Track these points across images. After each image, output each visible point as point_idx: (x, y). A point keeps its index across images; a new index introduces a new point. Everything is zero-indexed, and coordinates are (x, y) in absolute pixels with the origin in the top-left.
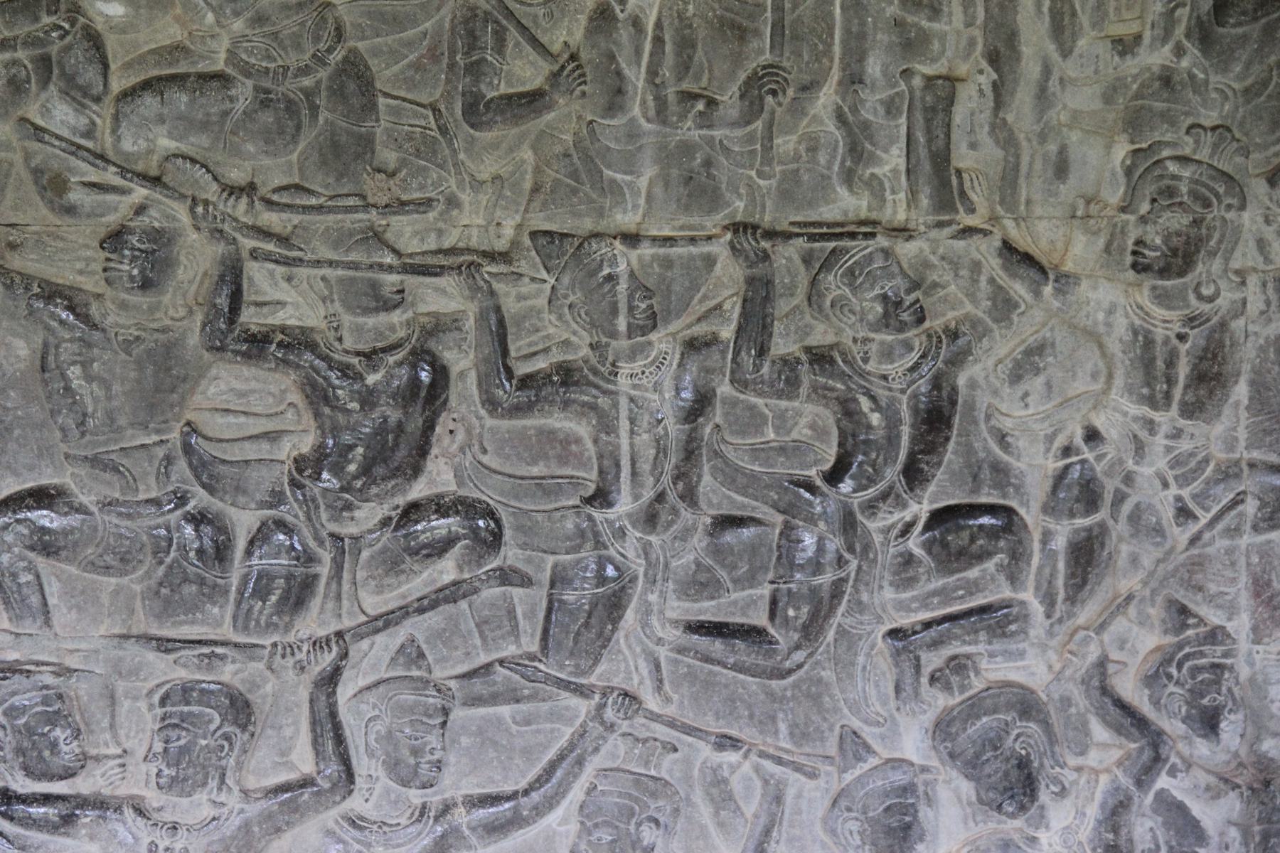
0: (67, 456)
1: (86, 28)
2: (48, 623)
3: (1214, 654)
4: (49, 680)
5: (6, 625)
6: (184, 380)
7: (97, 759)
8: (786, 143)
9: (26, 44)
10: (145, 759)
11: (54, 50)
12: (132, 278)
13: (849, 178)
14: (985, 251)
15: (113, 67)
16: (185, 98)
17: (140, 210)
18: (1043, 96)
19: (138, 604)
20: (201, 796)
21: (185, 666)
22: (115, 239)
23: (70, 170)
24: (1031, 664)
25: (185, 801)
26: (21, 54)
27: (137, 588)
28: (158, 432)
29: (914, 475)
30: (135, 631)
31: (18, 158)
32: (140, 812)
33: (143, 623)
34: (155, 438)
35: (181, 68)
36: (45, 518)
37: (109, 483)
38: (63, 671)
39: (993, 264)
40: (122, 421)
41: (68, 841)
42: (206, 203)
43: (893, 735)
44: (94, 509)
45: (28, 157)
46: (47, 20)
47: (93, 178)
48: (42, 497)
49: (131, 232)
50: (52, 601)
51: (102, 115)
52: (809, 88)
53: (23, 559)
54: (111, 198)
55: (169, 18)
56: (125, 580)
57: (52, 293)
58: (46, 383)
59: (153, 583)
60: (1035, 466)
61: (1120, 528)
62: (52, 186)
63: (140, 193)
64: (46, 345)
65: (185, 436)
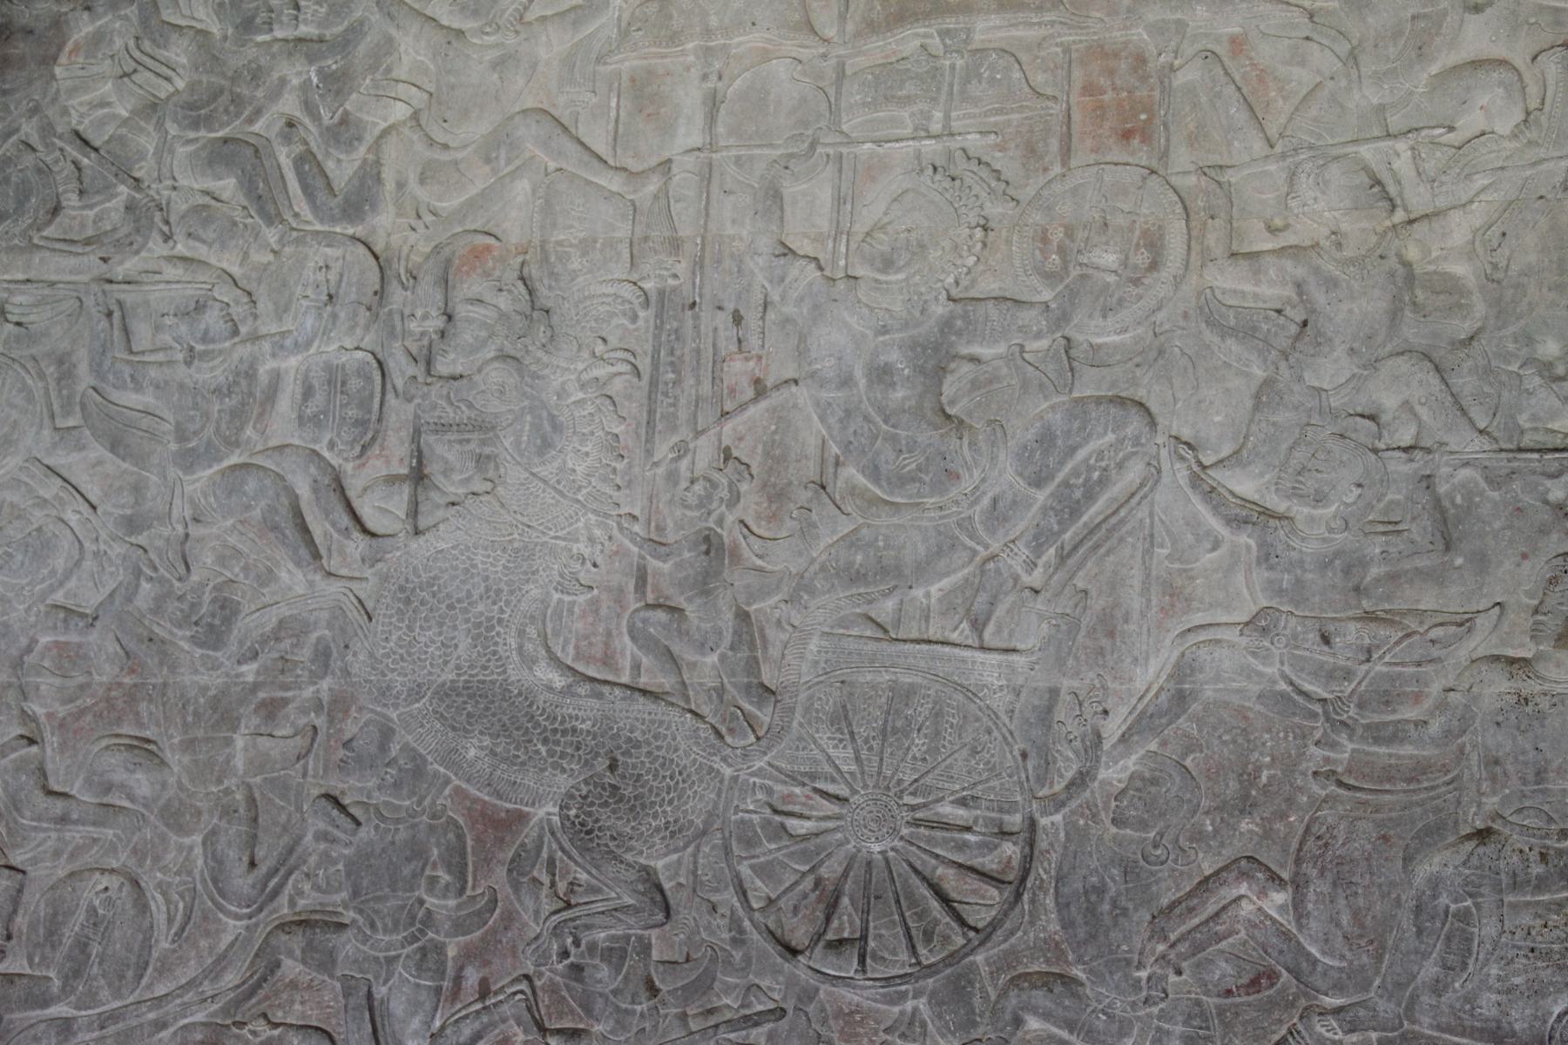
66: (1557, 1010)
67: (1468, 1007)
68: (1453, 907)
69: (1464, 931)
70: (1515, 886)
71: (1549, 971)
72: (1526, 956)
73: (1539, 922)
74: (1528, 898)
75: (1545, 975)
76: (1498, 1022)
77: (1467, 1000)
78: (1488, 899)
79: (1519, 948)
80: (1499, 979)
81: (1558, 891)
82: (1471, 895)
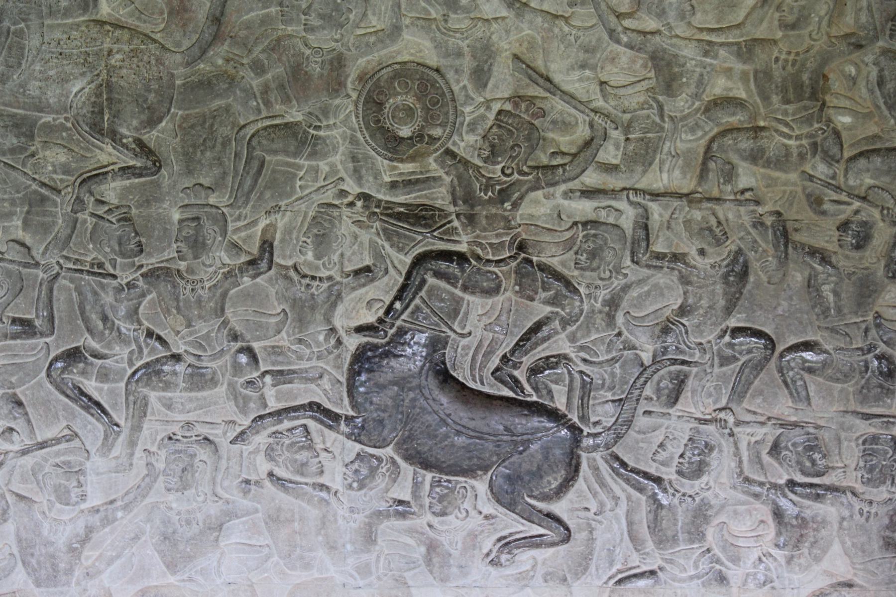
0: (819, 327)
1: (834, 129)
2: (809, 404)
4: (812, 430)
5: (791, 404)
6: (876, 291)
7: (833, 468)
9: (806, 137)
10: (855, 469)
11: (819, 140)
12: (852, 244)
15: (845, 146)
16: (879, 160)
17: (857, 212)
19: (851, 397)
20: (883, 488)
21: (875, 426)
22: (844, 226)
23: (825, 195)
25: (875, 490)
26: (804, 142)
27: (851, 389)
28: (862, 316)
30: (850, 409)
31: (799, 189)
32: (854, 494)
33: (853, 406)
34: (861, 319)
35: (878, 146)
36: (808, 355)
37: (838, 340)
38: (818, 427)
40: (846, 311)
41: (821, 506)
42: (888, 209)
44: (832, 352)
45: (804, 189)
46: (816, 126)
47: (835, 198)
48: (807, 346)
49: (852, 222)
50: (811, 394)
51: (840, 169)
53: (798, 374)
54: (842, 207)
55: (872, 123)
56: (845, 385)
57: (813, 252)
58: (809, 293)
59: (859, 387)
62: (815, 202)
63: (857, 204)
64: (810, 275)
65: (876, 318)
66: (75, 90)
67: (21, 90)
68: (13, 28)
69: (19, 43)
70: (51, 14)
71: (70, 66)
72: (57, 58)
73: (65, 36)
74: (59, 21)
75: (68, 69)
76: (40, 98)
77: (21, 86)
78: (34, 23)
79: (53, 53)
80: (41, 72)
81: (77, 17)
82: (24, 20)
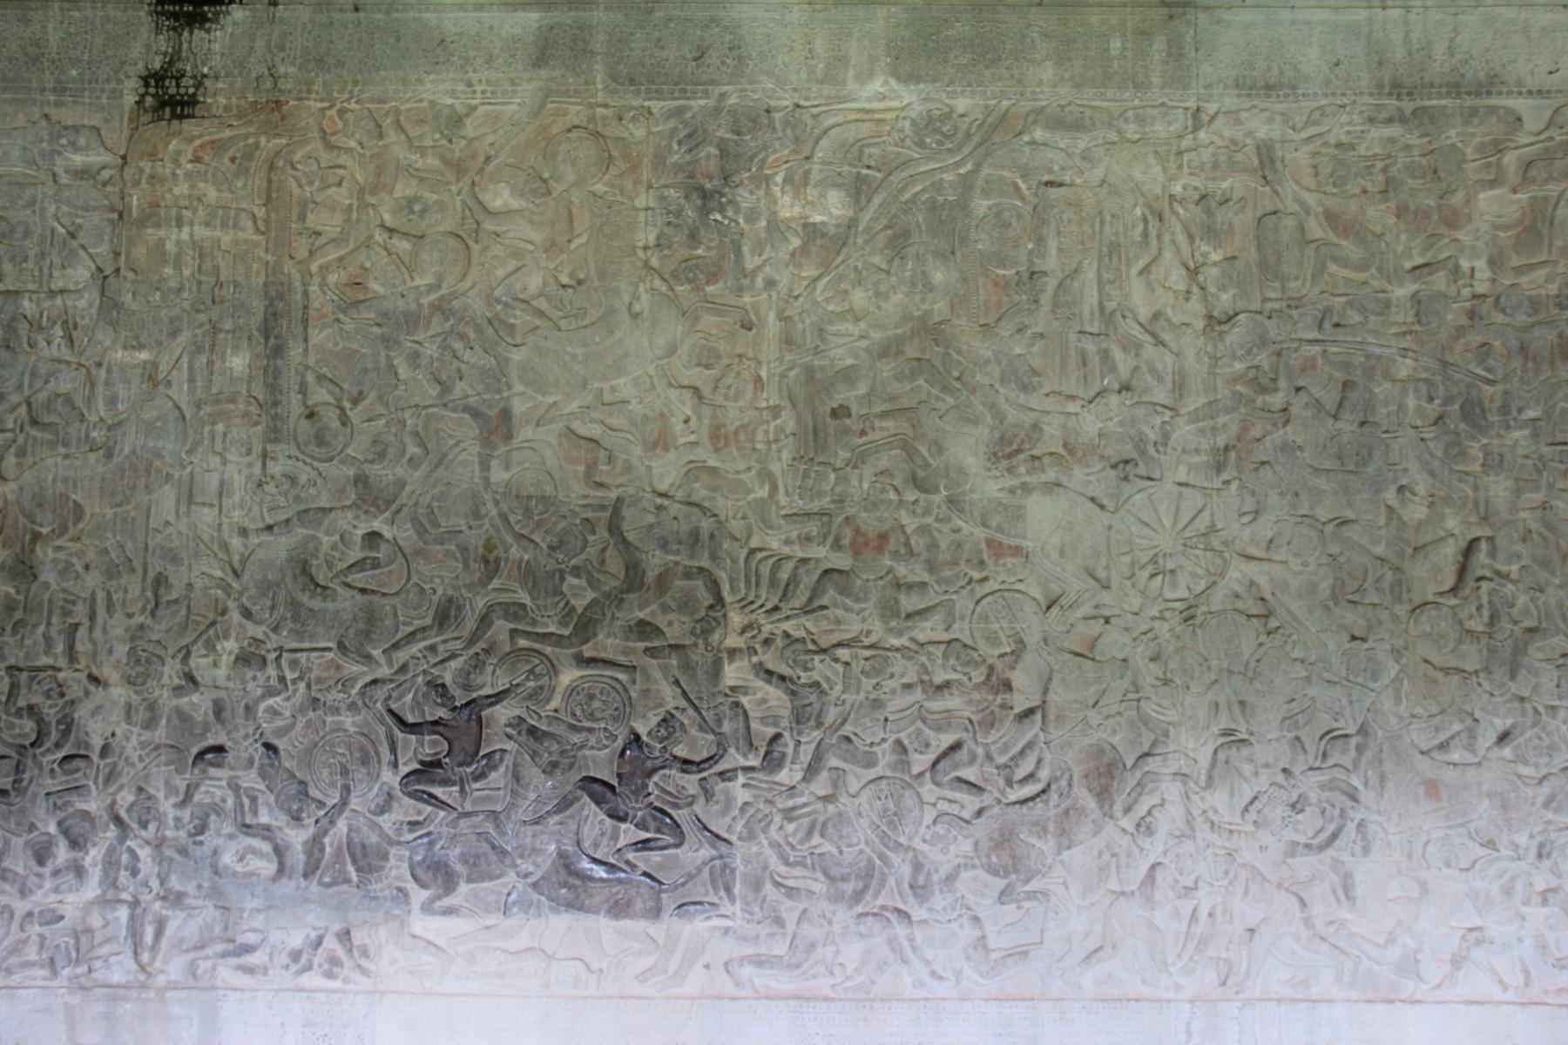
3: (149, 803)
8: (28, 642)
13: (46, 653)
14: (83, 676)
18: (105, 630)
24: (93, 804)
29: (58, 746)
39: (85, 681)
43: (47, 825)
52: (35, 626)
60: (97, 742)
61: (122, 764)
